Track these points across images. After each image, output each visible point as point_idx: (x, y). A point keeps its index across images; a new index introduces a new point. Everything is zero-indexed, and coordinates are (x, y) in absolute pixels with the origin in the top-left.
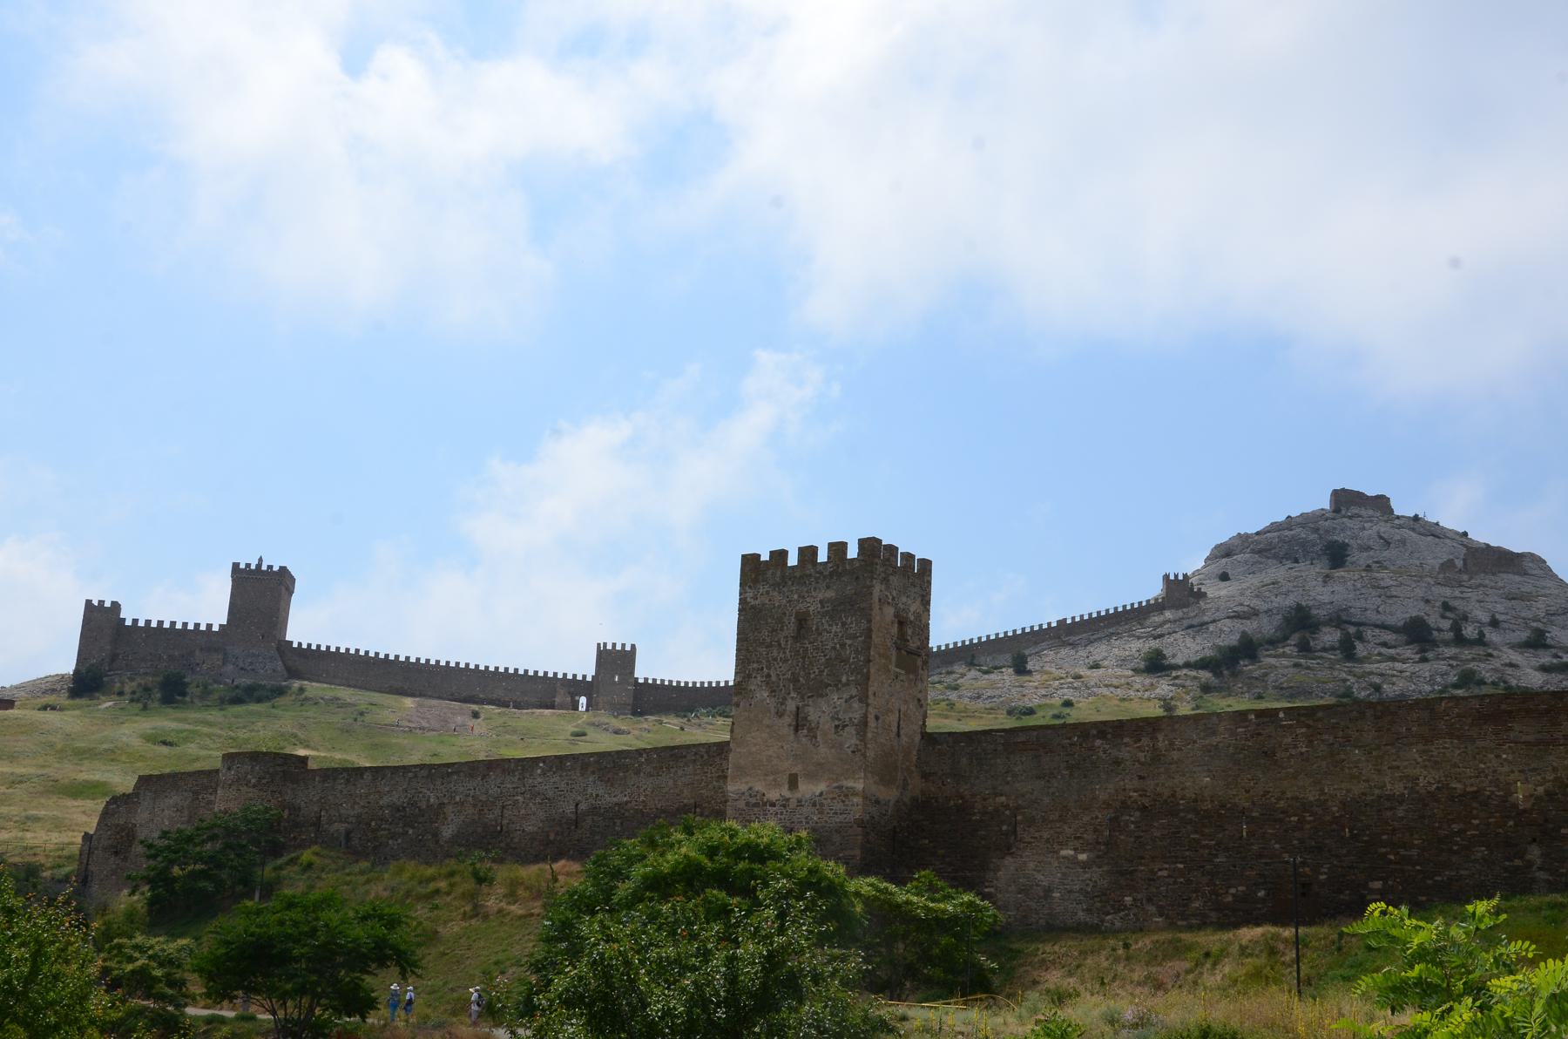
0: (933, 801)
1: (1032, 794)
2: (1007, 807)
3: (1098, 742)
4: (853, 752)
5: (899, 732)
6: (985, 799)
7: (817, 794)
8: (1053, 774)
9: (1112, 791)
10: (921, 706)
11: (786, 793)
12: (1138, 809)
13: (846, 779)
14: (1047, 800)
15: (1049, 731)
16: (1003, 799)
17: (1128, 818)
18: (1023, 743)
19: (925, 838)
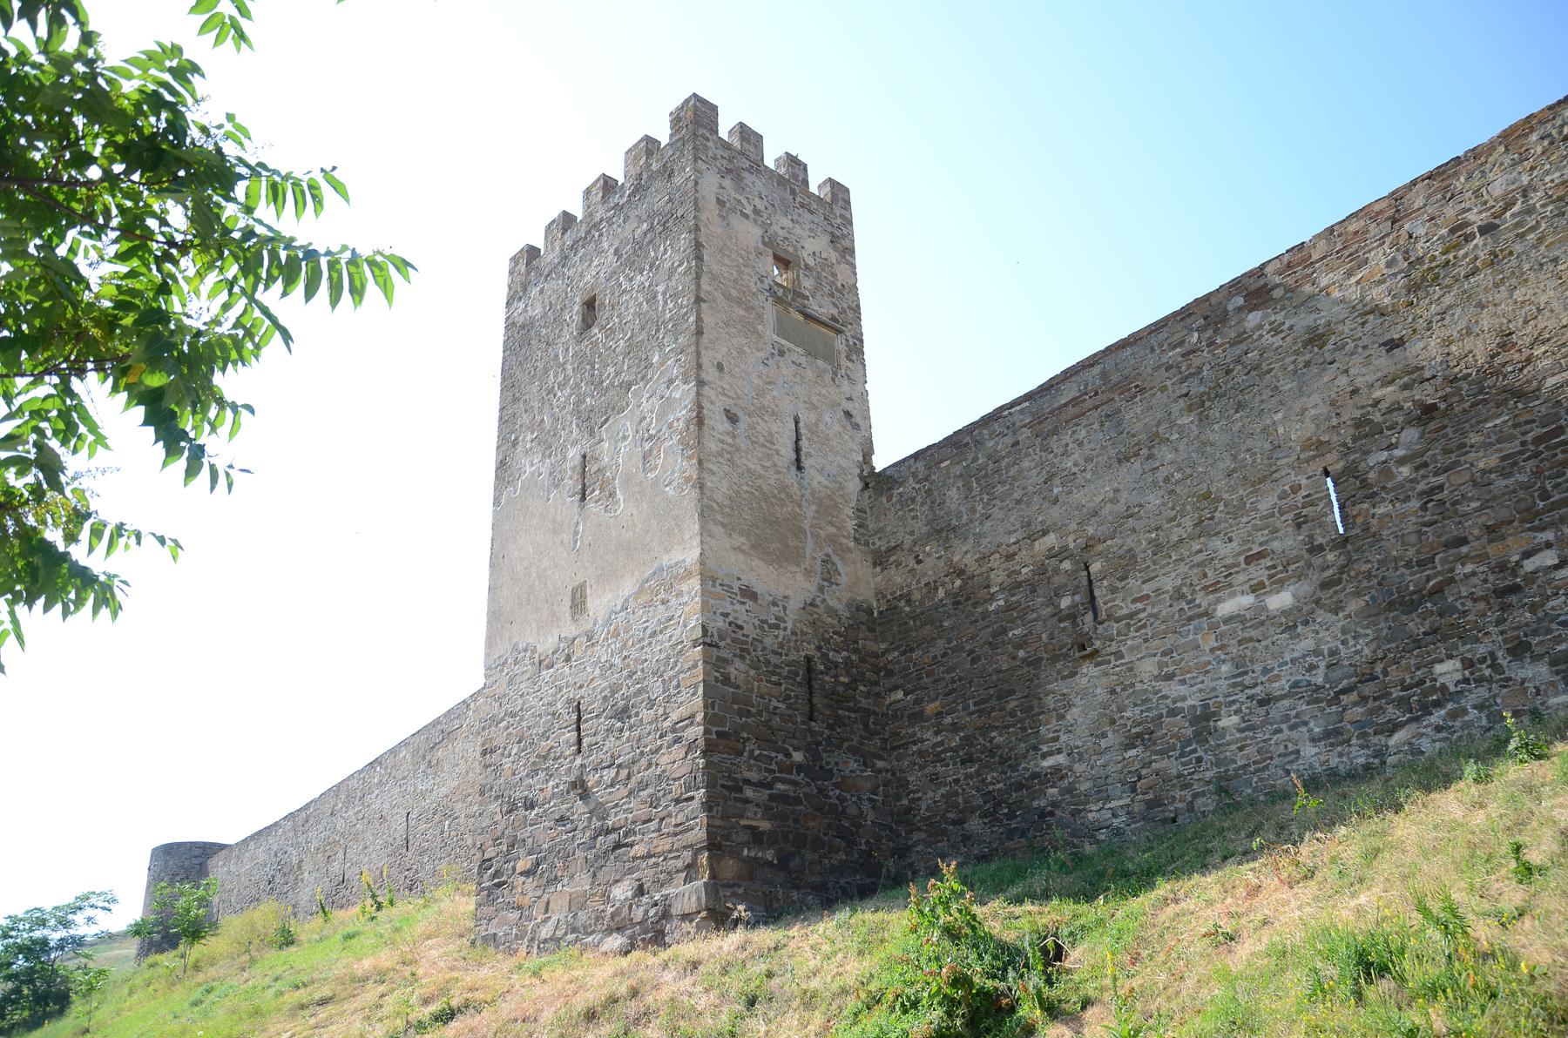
0: (903, 603)
1: (1114, 501)
2: (1059, 554)
3: (1254, 318)
5: (798, 460)
8: (1157, 434)
9: (1324, 410)
10: (856, 426)
11: (570, 630)
12: (1410, 421)
13: (667, 551)
14: (1154, 500)
15: (1129, 350)
16: (1051, 540)
17: (1384, 455)
18: (1075, 401)
19: (895, 688)
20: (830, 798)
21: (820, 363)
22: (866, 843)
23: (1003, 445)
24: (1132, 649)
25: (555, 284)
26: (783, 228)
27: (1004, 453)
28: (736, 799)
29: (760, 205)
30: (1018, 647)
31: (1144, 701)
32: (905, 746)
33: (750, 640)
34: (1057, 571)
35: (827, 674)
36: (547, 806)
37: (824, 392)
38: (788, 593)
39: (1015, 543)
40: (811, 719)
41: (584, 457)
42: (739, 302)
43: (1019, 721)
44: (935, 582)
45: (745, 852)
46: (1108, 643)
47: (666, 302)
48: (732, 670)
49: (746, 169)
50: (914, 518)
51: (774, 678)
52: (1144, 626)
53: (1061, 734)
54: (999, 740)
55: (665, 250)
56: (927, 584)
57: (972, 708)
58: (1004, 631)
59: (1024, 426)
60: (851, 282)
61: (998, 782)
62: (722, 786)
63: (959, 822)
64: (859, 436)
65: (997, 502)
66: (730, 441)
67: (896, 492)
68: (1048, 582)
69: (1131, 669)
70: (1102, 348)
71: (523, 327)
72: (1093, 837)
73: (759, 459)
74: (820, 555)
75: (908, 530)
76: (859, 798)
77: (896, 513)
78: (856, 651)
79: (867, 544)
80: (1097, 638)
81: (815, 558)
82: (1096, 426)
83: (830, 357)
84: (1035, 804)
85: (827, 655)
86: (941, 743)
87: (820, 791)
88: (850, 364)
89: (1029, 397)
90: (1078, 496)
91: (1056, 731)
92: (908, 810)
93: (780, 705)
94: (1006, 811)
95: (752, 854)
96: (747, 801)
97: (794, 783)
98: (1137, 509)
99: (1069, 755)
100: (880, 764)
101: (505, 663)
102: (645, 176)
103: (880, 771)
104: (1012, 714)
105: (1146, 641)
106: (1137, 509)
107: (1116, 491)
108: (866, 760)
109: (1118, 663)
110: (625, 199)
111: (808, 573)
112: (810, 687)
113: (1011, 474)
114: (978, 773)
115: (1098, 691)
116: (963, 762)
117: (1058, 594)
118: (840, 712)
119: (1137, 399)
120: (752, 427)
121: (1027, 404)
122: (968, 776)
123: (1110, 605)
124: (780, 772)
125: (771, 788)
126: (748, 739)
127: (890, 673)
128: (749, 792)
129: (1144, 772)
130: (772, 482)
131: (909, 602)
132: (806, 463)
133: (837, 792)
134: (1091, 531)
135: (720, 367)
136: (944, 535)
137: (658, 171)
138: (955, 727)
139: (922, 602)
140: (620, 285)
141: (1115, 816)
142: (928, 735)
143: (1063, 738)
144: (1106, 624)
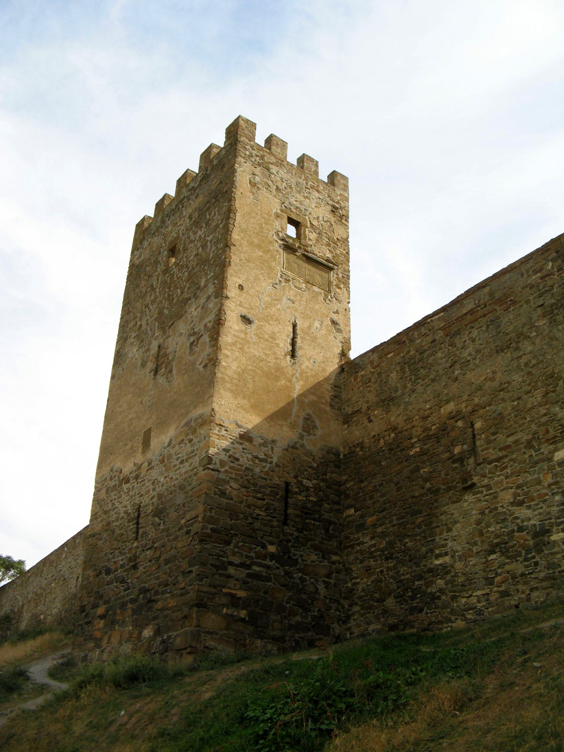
0: (358, 449)
1: (493, 379)
2: (456, 416)
4: (205, 366)
6: (425, 418)
7: (166, 444)
8: (522, 333)
10: (339, 331)
11: (139, 458)
13: (195, 407)
14: (517, 378)
15: (508, 276)
20: (294, 578)
21: (316, 289)
22: (318, 611)
23: (425, 342)
24: (497, 483)
25: (157, 240)
26: (296, 201)
27: (426, 348)
28: (221, 575)
30: (426, 480)
31: (505, 520)
32: (352, 546)
33: (244, 468)
34: (454, 428)
35: (300, 494)
36: (116, 573)
37: (317, 307)
38: (275, 438)
39: (429, 409)
40: (285, 523)
41: (159, 347)
42: (259, 247)
43: (423, 532)
44: (379, 435)
45: (225, 610)
46: (483, 479)
47: (212, 247)
48: (228, 487)
50: (370, 391)
51: (258, 495)
52: (506, 467)
53: (448, 542)
54: (410, 544)
55: (215, 214)
56: (374, 436)
57: (395, 522)
58: (418, 469)
59: (440, 329)
60: (345, 236)
61: (407, 573)
62: (212, 565)
63: (381, 600)
64: (340, 337)
65: (420, 381)
66: (242, 336)
67: (360, 374)
68: (448, 436)
69: (496, 497)
70: (491, 275)
71: (137, 266)
72: (464, 615)
73: (263, 349)
74: (303, 414)
75: (365, 399)
76: (316, 580)
77: (359, 388)
78: (324, 480)
79: (339, 409)
80: (475, 475)
81: (298, 417)
82: (484, 328)
83: (328, 288)
84: (429, 590)
85: (302, 482)
86: (374, 545)
87: (287, 573)
88: (338, 290)
89: (444, 309)
90: (470, 376)
91: (446, 540)
92: (351, 590)
93: (262, 513)
94: (410, 594)
95: (230, 612)
96: (229, 576)
97: (268, 567)
98: (506, 385)
99: (452, 556)
100: (334, 558)
101: (106, 479)
102: (209, 169)
103: (334, 563)
104: (419, 527)
105: (507, 477)
106: (506, 385)
107: (494, 372)
108: (325, 554)
109: (488, 492)
110: (198, 183)
111: (293, 426)
112: (286, 503)
113: (430, 361)
114: (395, 567)
115: (474, 512)
116: (387, 559)
117: (453, 444)
118: (307, 521)
119: (511, 309)
120: (260, 327)
121: (442, 314)
122: (389, 569)
123: (485, 452)
124: (257, 558)
125: (249, 569)
126: (236, 534)
127: (347, 497)
128: (231, 570)
129: (499, 571)
130: (272, 364)
131: (362, 448)
132: (299, 353)
133: (300, 575)
134: (476, 400)
135: (241, 287)
136: (386, 402)
137: (216, 165)
138: (383, 535)
139: (369, 447)
140: (189, 237)
141: (479, 601)
142: (367, 539)
143: (450, 544)
144: (482, 466)
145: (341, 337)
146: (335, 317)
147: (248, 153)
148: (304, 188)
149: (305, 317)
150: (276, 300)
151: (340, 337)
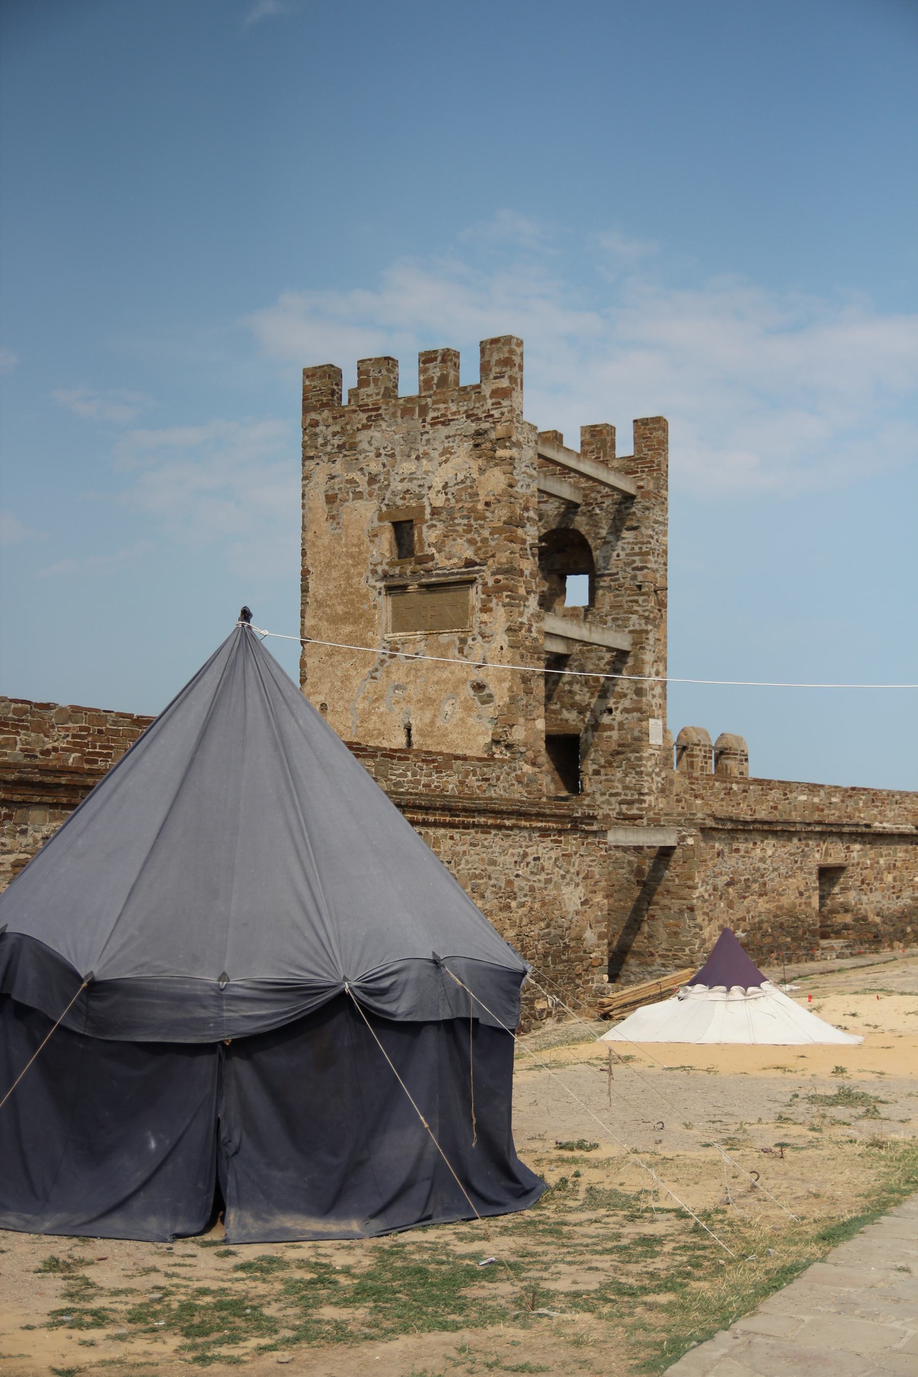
26: (402, 481)
29: (374, 467)
49: (366, 427)
64: (490, 710)
145: (491, 710)
146: (478, 676)
147: (320, 441)
148: (419, 437)
149: (428, 702)
150: (377, 700)
151: (490, 710)
